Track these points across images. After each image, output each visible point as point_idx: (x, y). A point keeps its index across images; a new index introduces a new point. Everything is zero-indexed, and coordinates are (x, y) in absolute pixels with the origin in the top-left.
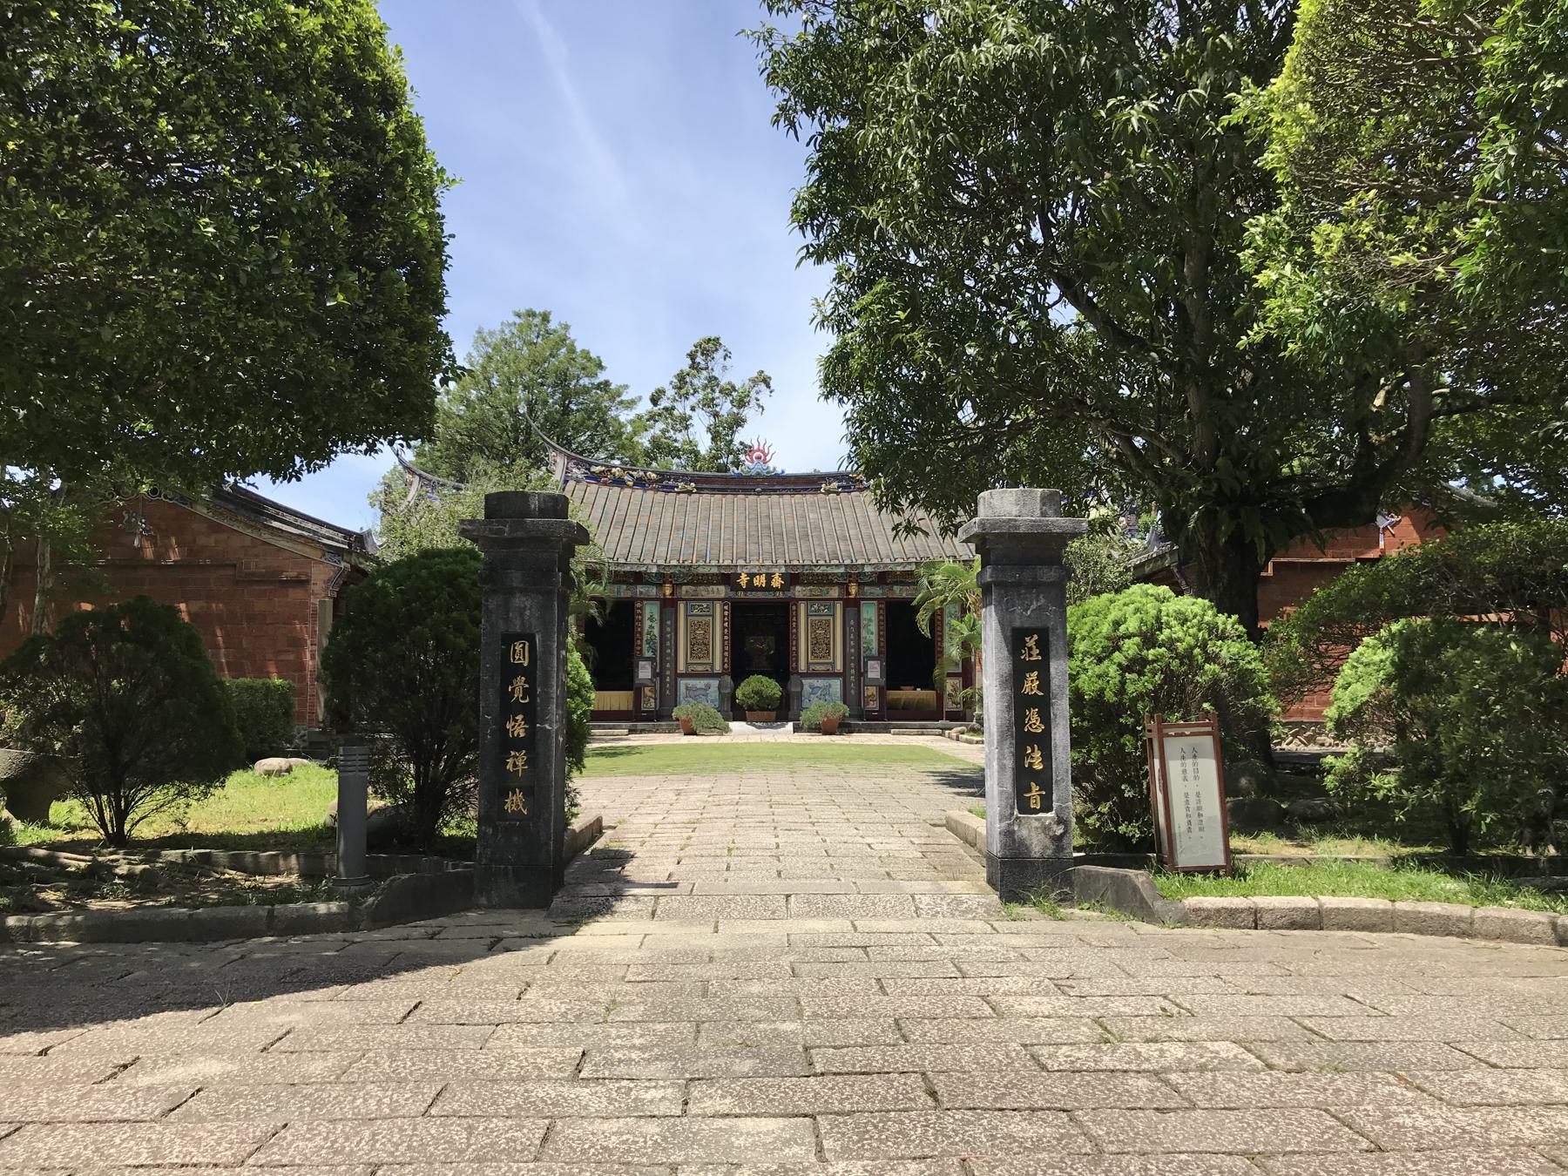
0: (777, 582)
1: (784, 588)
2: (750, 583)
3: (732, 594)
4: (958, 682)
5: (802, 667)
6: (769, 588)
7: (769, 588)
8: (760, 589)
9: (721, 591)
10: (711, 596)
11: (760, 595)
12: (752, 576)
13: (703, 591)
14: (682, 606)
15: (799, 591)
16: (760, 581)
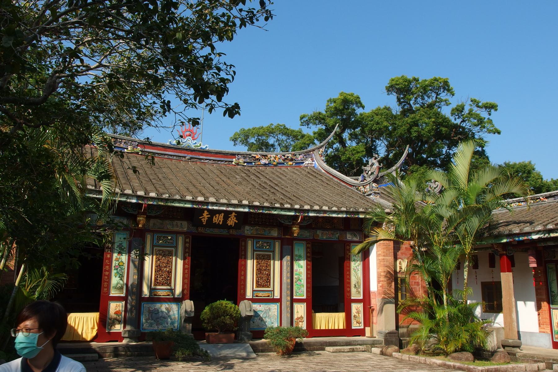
0: (232, 221)
1: (237, 226)
2: (210, 220)
3: (194, 230)
4: (360, 306)
5: (249, 294)
6: (224, 225)
7: (224, 225)
8: (217, 226)
9: (184, 226)
10: (175, 229)
11: (216, 231)
12: (213, 213)
13: (169, 225)
14: (149, 238)
15: (248, 230)
16: (218, 219)
